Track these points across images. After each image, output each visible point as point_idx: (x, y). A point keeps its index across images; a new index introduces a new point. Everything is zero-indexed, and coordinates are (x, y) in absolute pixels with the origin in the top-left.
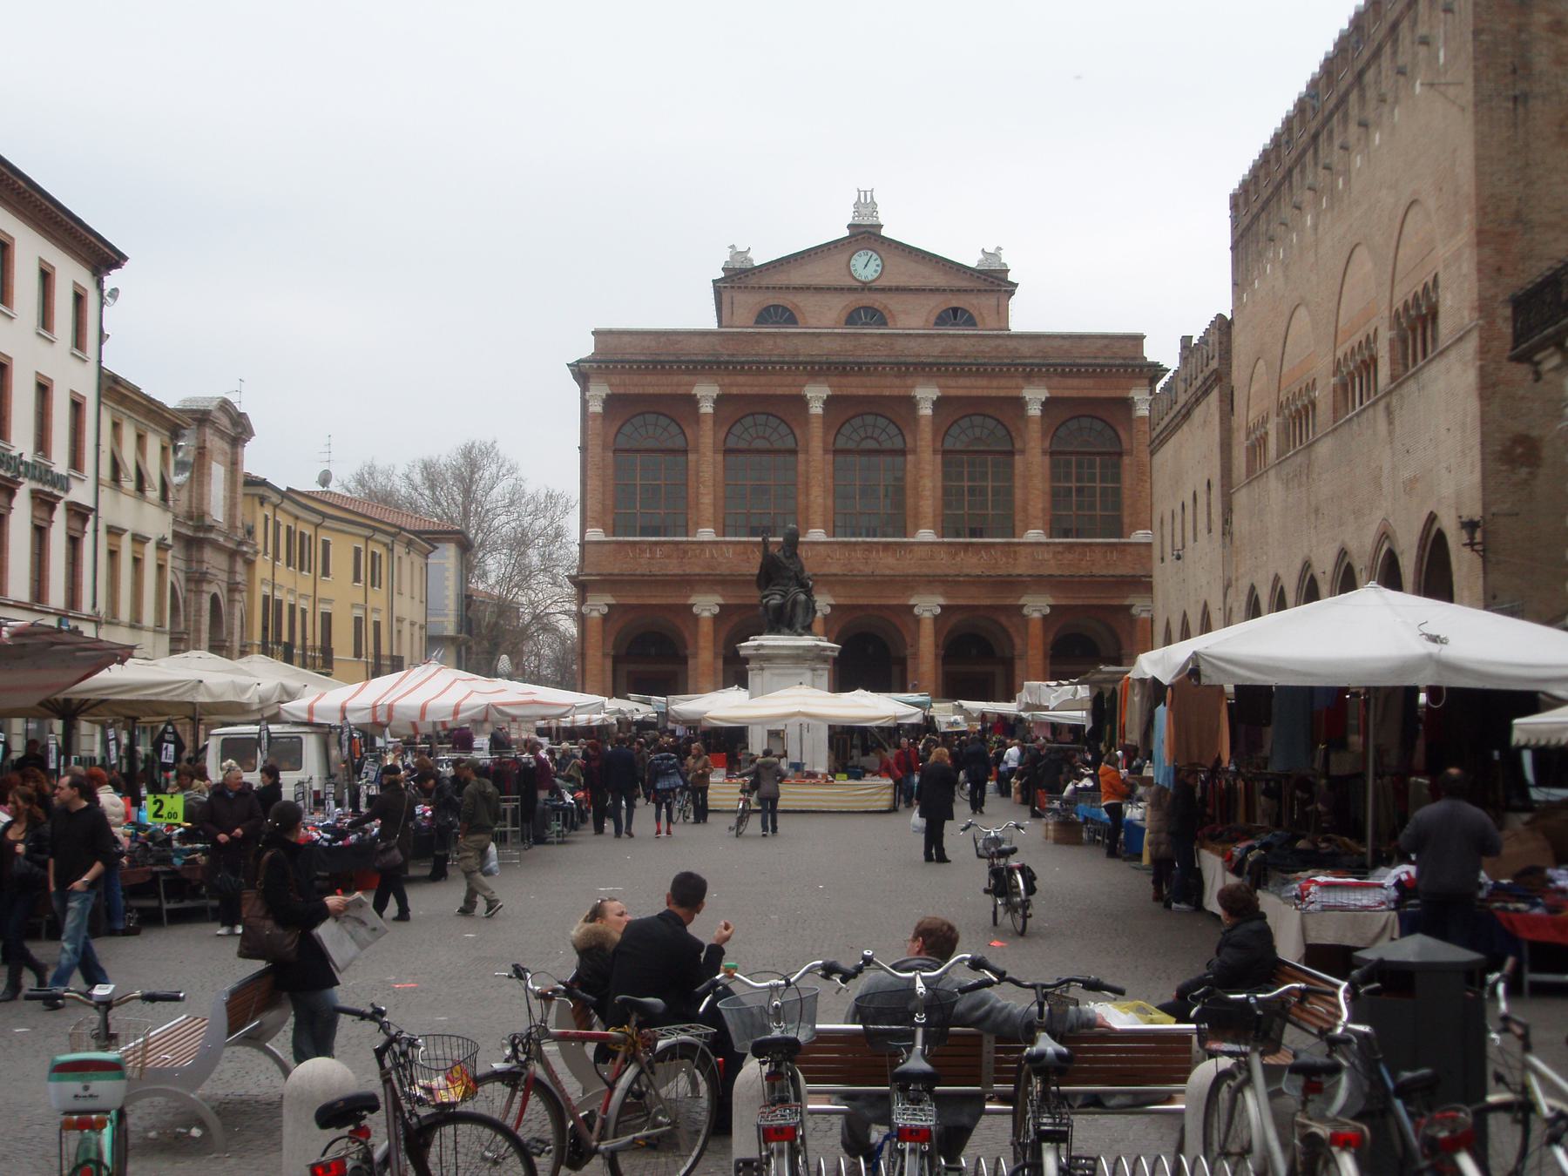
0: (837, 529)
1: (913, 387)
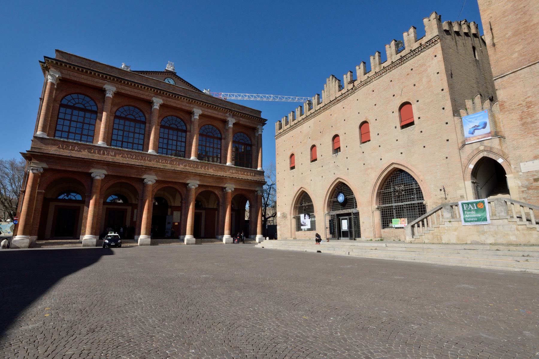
1: (193, 108)
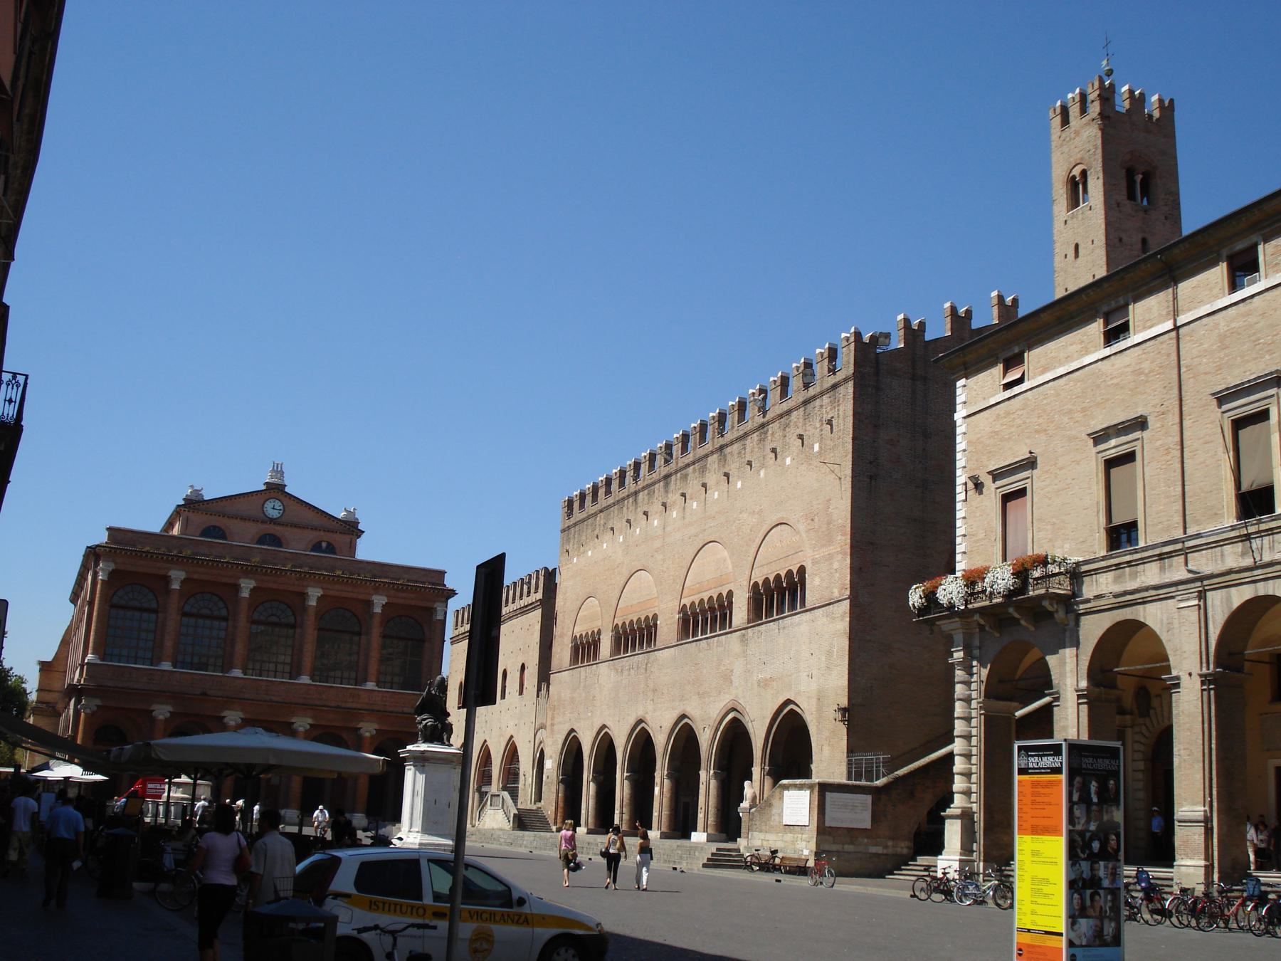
0: (278, 673)
